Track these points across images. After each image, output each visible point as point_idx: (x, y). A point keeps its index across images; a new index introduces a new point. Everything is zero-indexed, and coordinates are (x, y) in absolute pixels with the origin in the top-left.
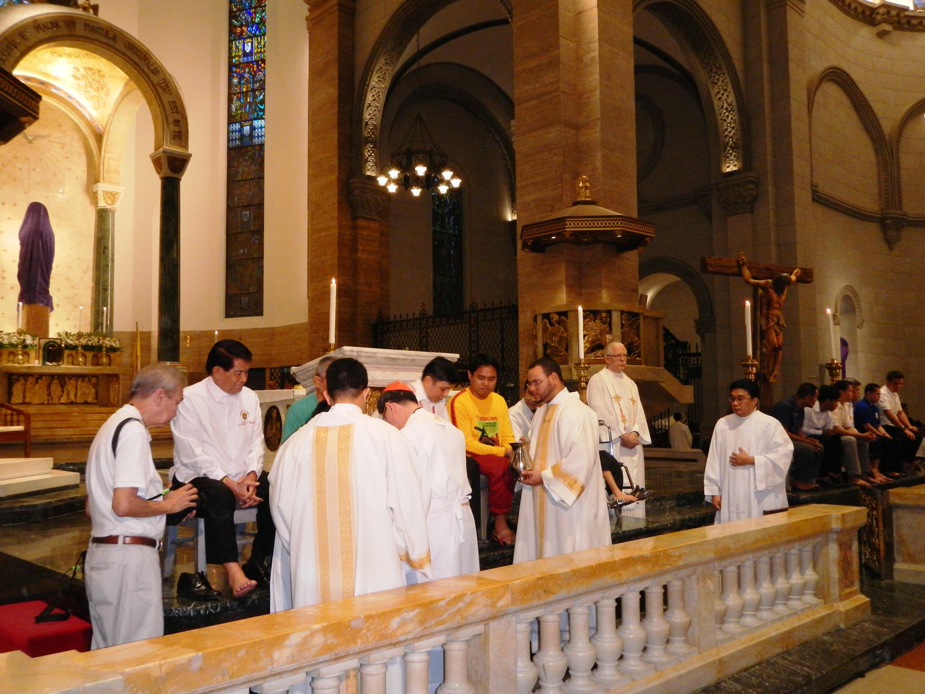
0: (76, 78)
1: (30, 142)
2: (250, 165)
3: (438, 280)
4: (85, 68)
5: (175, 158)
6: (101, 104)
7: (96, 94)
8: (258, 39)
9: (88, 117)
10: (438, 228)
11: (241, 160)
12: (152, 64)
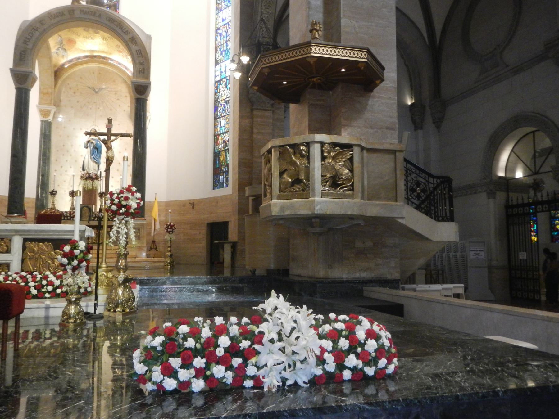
0: (120, 52)
1: (97, 92)
12: (125, 28)
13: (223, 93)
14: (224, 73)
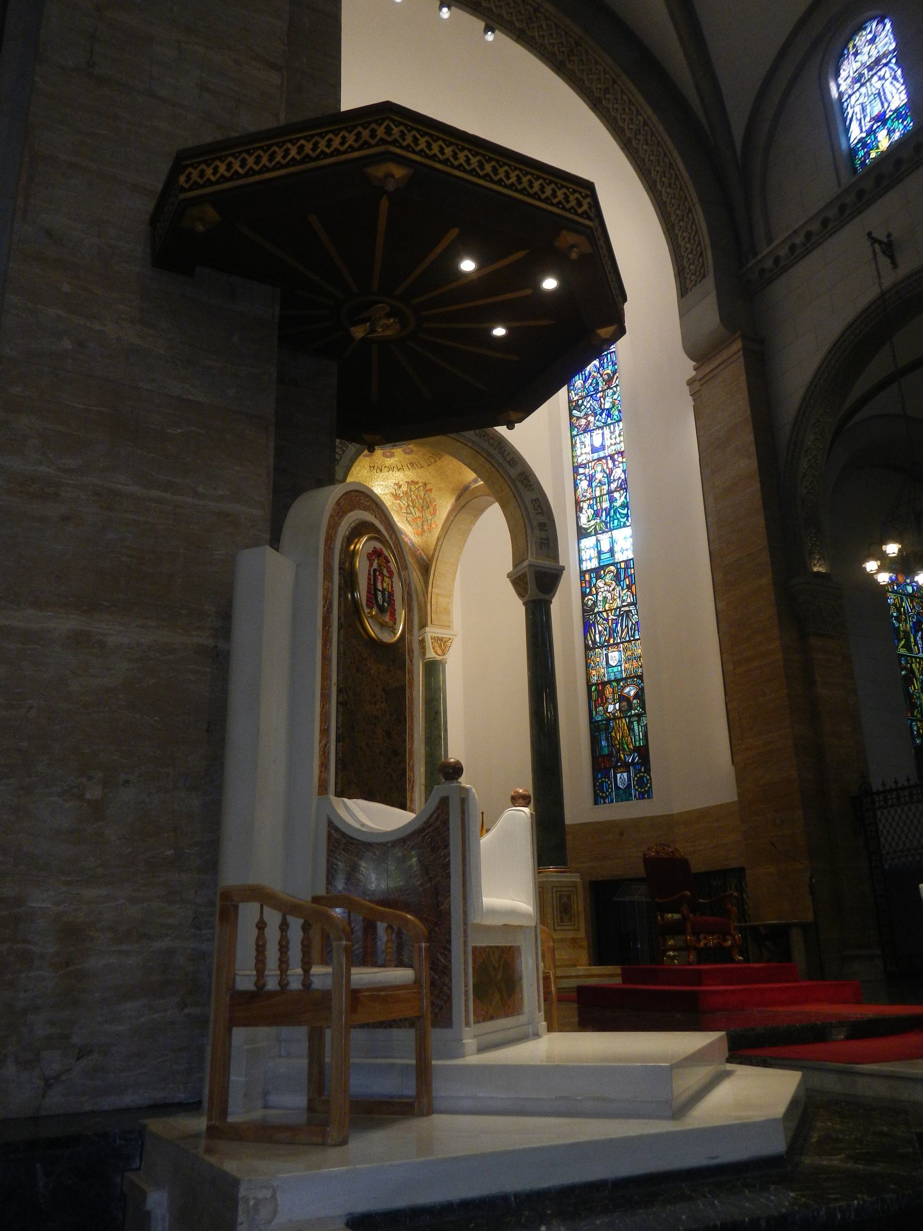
0: (396, 496)
2: (613, 590)
3: (915, 728)
4: (408, 483)
5: (545, 574)
6: (425, 527)
7: (418, 514)
8: (610, 428)
9: (410, 544)
10: (902, 651)
11: (600, 584)
13: (609, 595)
14: (608, 555)
